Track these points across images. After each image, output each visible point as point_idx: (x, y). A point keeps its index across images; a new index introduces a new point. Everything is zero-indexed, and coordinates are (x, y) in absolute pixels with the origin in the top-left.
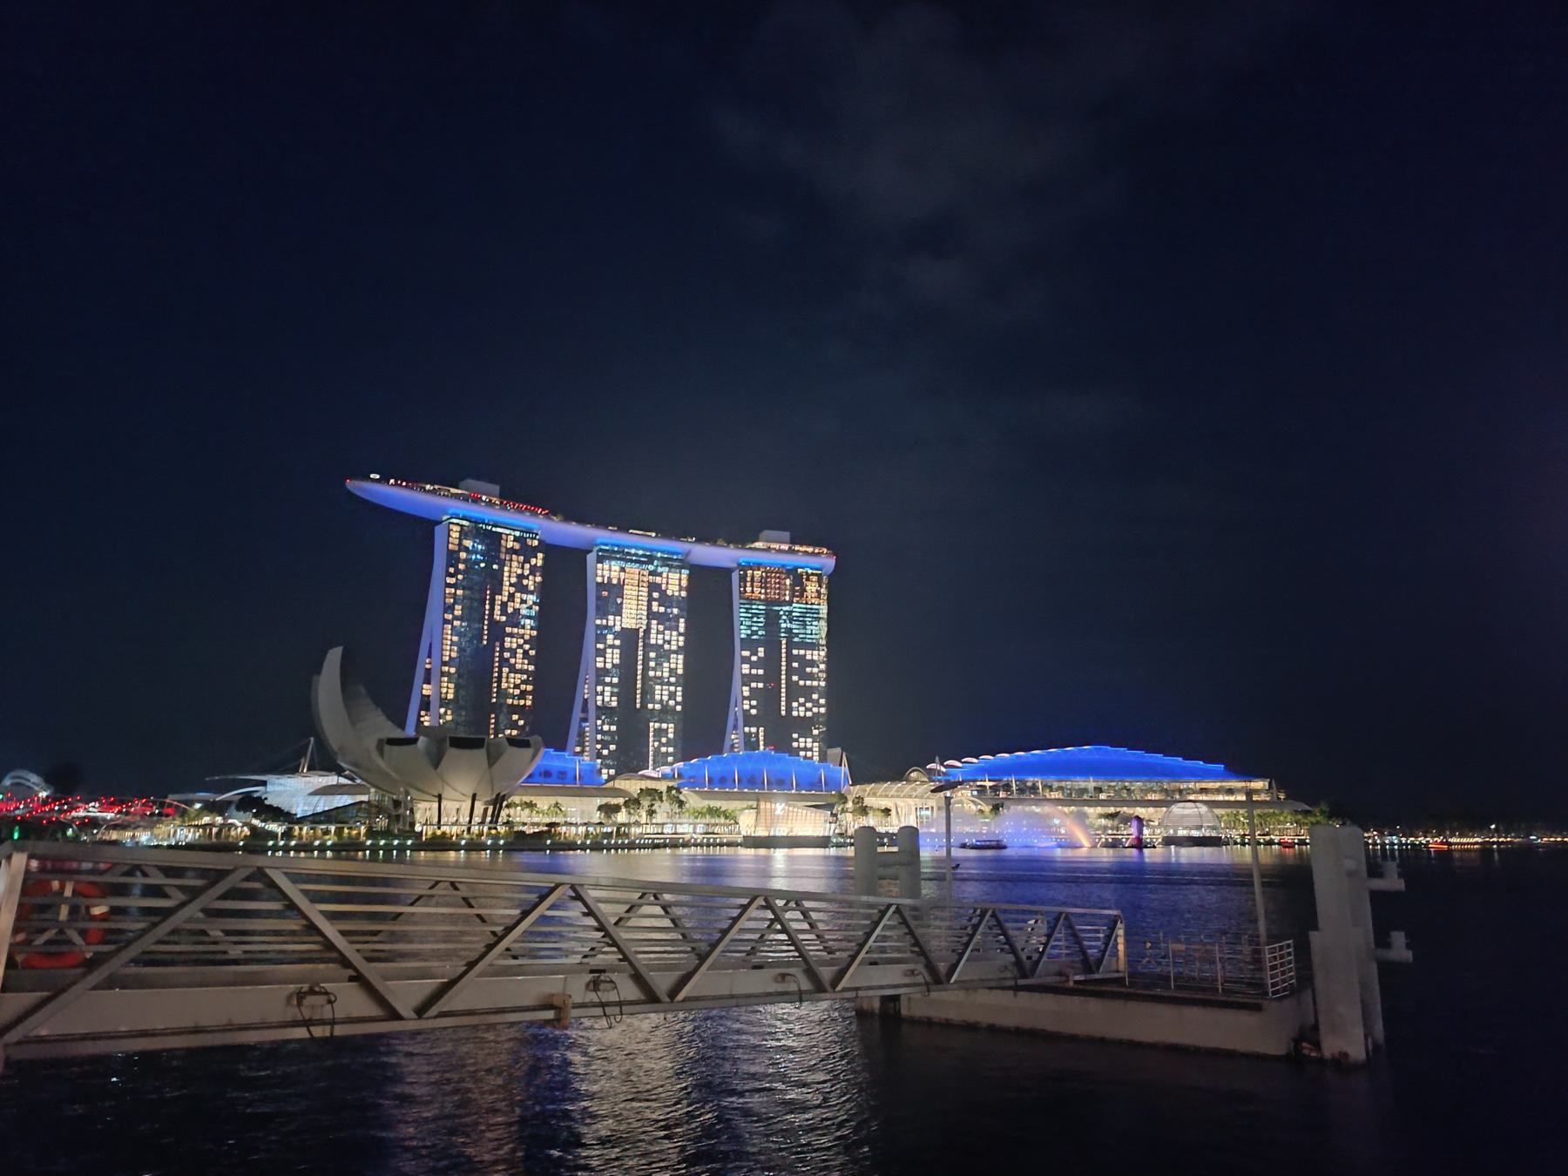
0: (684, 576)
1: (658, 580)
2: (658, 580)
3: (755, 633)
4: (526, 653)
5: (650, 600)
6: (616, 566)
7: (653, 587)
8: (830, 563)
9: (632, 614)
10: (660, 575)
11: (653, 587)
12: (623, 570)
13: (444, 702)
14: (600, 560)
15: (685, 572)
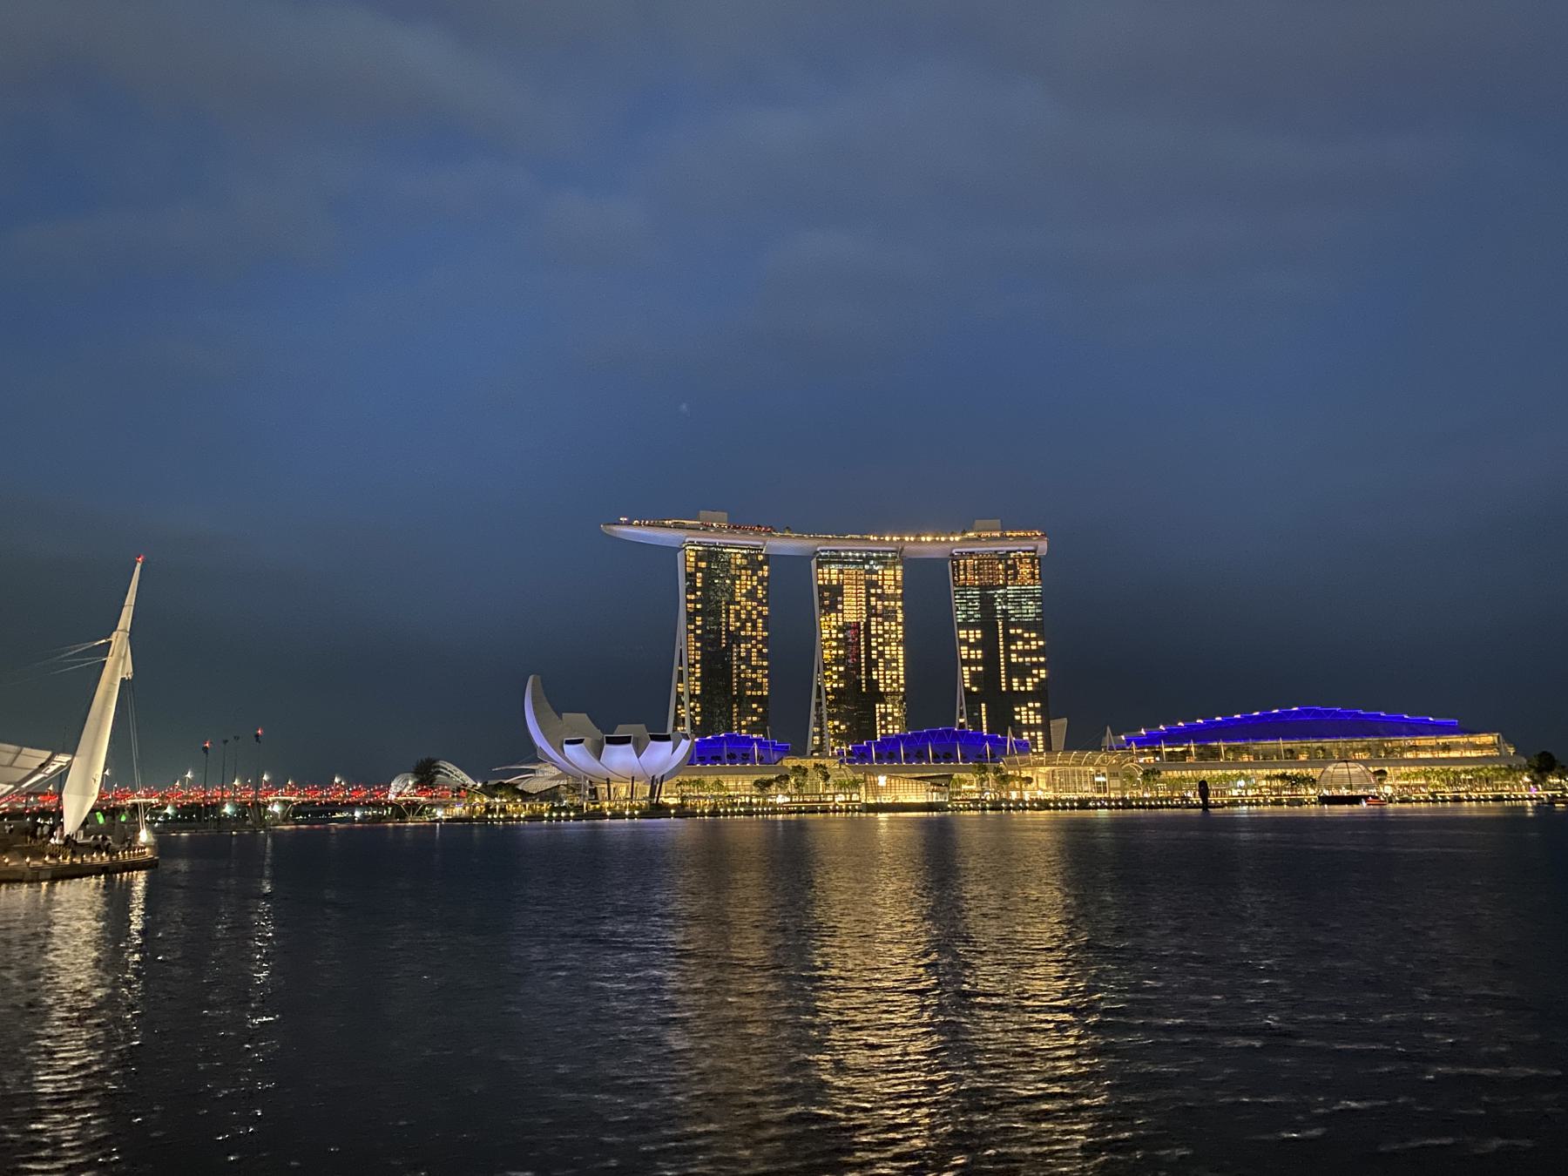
0: (899, 573)
1: (874, 577)
2: (874, 577)
3: (972, 617)
4: (760, 651)
5: (869, 595)
6: (834, 569)
7: (871, 584)
8: (1043, 546)
9: (852, 610)
10: (876, 573)
11: (871, 584)
12: (841, 571)
13: (692, 697)
14: (820, 565)
15: (899, 567)
